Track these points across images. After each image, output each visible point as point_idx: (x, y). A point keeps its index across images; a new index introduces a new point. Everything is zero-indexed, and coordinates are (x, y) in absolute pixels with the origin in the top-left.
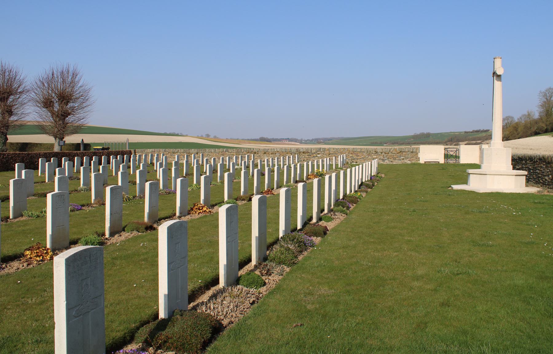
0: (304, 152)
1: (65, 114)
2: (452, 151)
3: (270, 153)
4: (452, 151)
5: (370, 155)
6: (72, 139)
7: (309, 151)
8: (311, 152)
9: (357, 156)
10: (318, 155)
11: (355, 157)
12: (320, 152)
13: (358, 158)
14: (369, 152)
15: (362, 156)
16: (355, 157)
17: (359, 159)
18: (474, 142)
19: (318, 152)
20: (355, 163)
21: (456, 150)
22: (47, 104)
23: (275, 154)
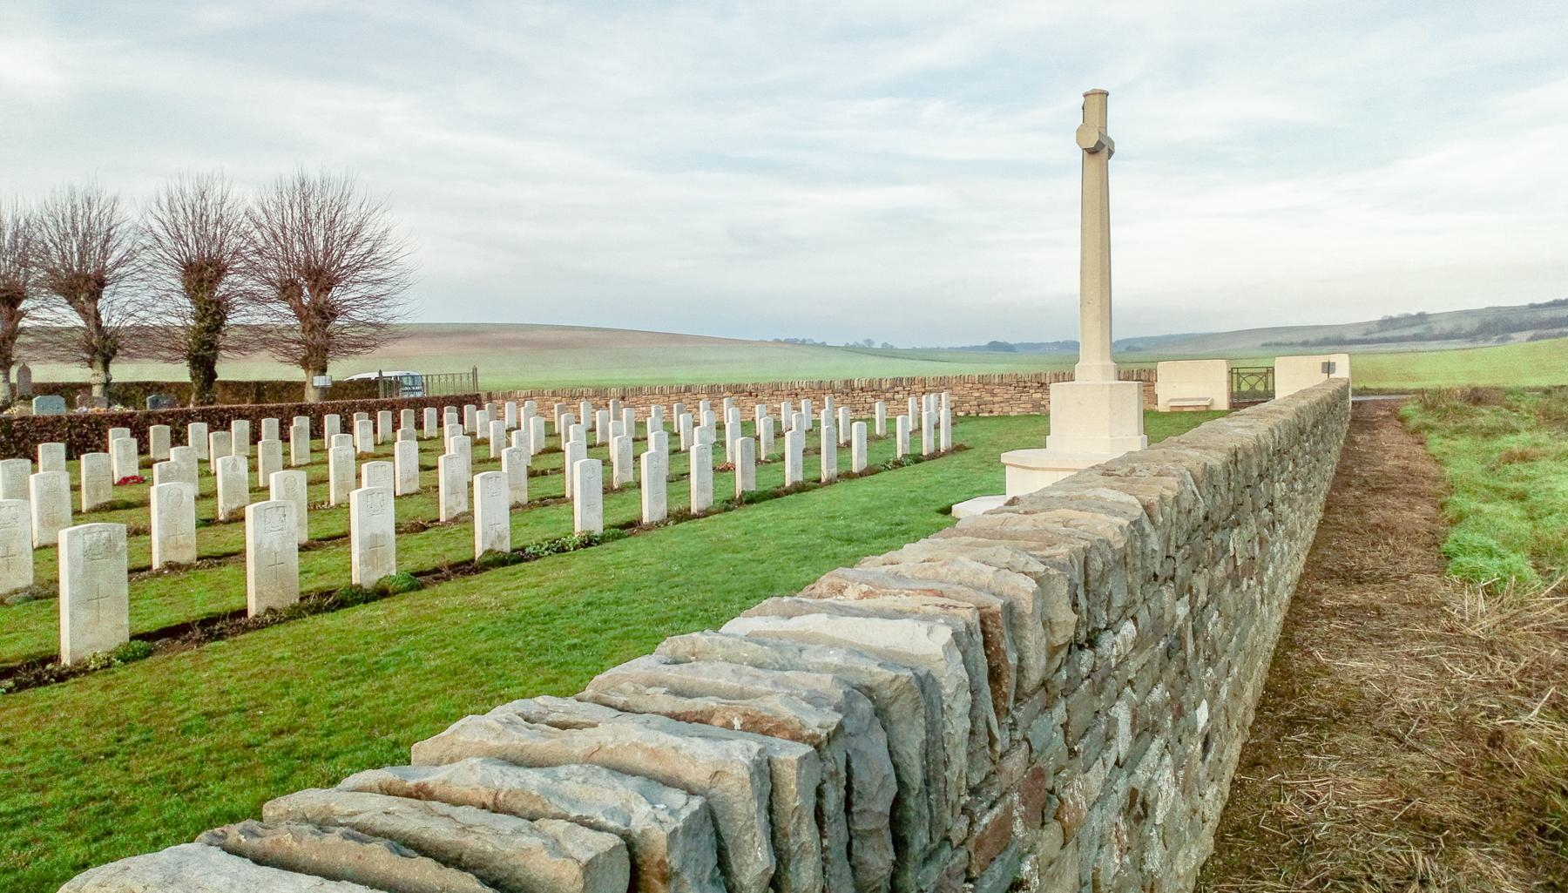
0: (862, 389)
1: (327, 313)
2: (1252, 374)
3: (785, 393)
4: (1252, 374)
5: (1023, 392)
6: (342, 369)
7: (876, 387)
8: (880, 385)
9: (993, 395)
10: (897, 396)
11: (988, 398)
12: (900, 388)
13: (996, 399)
14: (1022, 384)
15: (1006, 396)
16: (988, 398)
17: (998, 403)
18: (1557, 331)
19: (896, 389)
20: (987, 415)
21: (1265, 370)
22: (287, 290)
23: (796, 395)
